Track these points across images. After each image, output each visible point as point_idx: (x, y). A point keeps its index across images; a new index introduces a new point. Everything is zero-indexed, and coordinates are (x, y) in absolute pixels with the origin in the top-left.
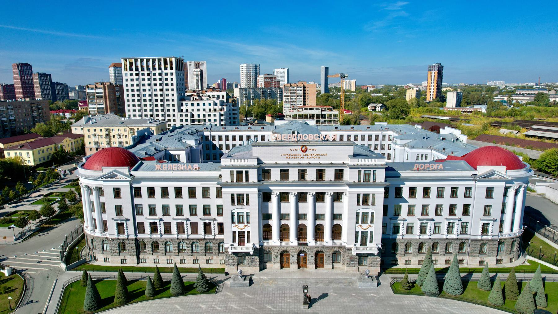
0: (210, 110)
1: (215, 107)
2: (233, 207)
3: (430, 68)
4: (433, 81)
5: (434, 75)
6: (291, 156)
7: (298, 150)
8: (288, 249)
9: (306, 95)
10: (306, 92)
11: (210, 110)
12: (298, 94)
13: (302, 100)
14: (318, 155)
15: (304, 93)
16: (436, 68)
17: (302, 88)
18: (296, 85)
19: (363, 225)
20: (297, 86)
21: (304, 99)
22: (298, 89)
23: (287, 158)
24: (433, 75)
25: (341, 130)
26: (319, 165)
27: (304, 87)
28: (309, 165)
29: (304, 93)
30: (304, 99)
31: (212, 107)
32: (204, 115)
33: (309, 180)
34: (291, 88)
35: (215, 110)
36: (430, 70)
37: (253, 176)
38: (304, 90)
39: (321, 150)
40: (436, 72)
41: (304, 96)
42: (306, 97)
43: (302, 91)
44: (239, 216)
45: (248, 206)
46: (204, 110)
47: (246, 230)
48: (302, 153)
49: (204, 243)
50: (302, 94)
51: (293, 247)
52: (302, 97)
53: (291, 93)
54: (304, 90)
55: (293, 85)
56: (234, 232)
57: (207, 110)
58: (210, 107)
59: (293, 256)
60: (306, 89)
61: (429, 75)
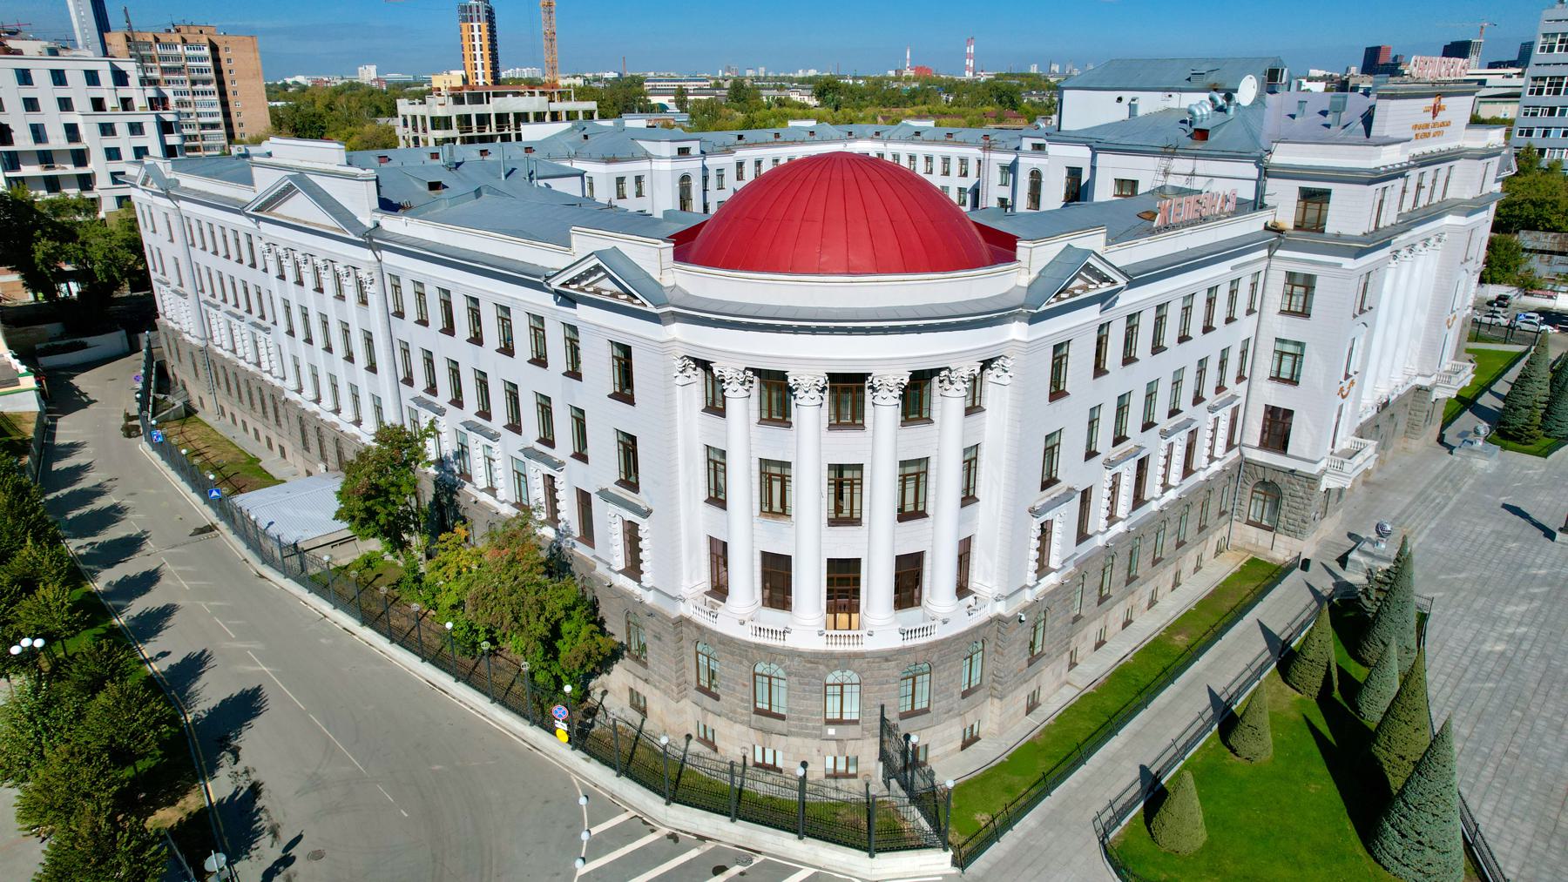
0: (98, 104)
1: (123, 92)
3: (466, 14)
4: (478, 52)
5: (479, 29)
6: (1432, 131)
9: (226, 75)
10: (225, 66)
11: (98, 104)
12: (196, 75)
13: (216, 98)
15: (219, 72)
16: (483, 14)
17: (207, 51)
18: (177, 38)
20: (184, 41)
21: (223, 93)
22: (191, 53)
24: (476, 33)
25: (755, 144)
27: (214, 49)
29: (219, 72)
30: (223, 93)
31: (107, 90)
32: (72, 131)
34: (159, 50)
35: (126, 104)
36: (465, 20)
38: (216, 61)
40: (484, 25)
41: (221, 83)
42: (229, 87)
43: (209, 64)
46: (65, 104)
50: (212, 75)
52: (213, 87)
53: (164, 70)
54: (216, 61)
55: (163, 39)
57: (82, 103)
58: (96, 92)
60: (222, 55)
61: (465, 34)
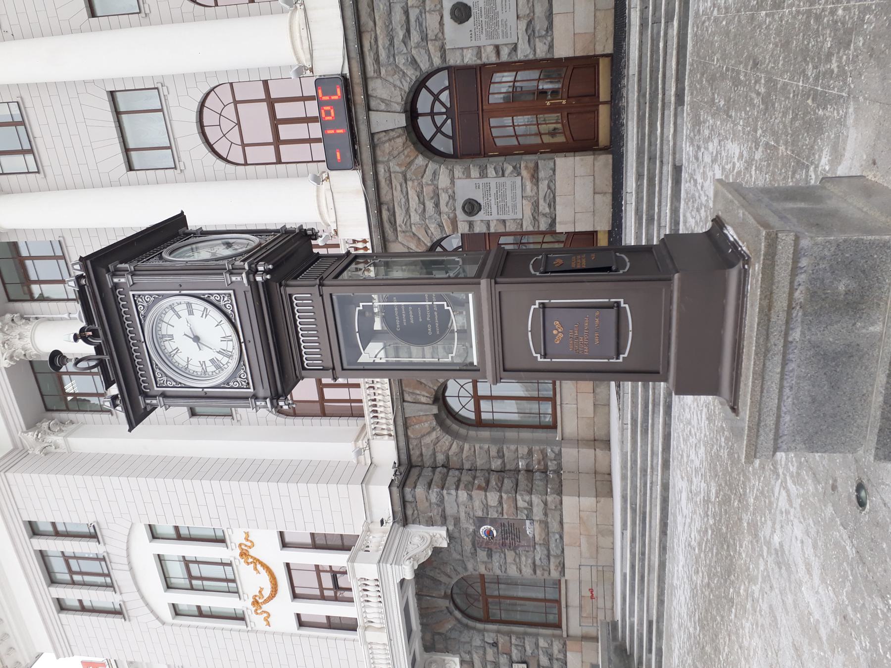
44: (194, 582)
45: (105, 532)
59: (472, 207)
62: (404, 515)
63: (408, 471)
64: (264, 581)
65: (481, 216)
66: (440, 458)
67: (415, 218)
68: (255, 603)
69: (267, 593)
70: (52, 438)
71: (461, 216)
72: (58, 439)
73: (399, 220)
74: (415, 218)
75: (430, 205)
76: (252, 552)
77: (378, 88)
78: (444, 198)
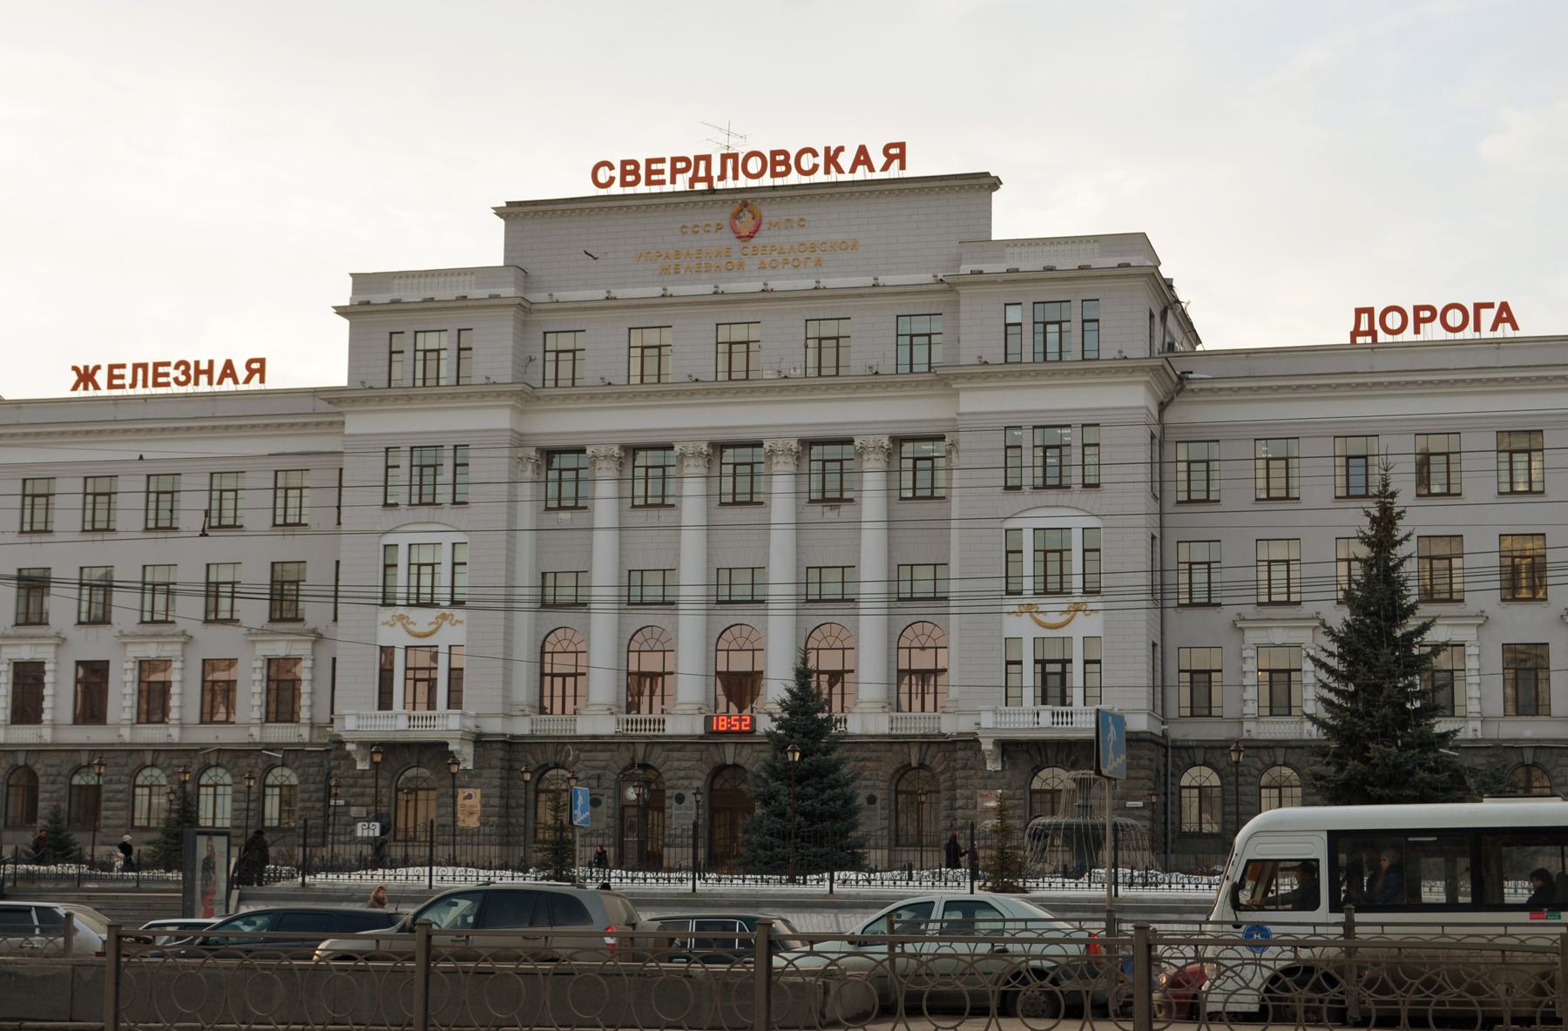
2: (388, 519)
7: (719, 227)
8: (656, 758)
14: (813, 248)
19: (1046, 603)
23: (664, 271)
26: (818, 293)
28: (767, 295)
33: (768, 374)
37: (494, 353)
39: (825, 224)
47: (442, 640)
48: (736, 245)
49: (257, 772)
51: (679, 744)
56: (387, 652)
59: (680, 799)
62: (481, 741)
63: (511, 744)
64: (422, 627)
65: (675, 804)
66: (517, 765)
67: (676, 764)
68: (402, 617)
69: (411, 627)
70: (530, 467)
71: (676, 792)
72: (528, 474)
73: (676, 755)
74: (676, 764)
75: (682, 774)
76: (446, 624)
77: (746, 751)
78: (686, 783)
